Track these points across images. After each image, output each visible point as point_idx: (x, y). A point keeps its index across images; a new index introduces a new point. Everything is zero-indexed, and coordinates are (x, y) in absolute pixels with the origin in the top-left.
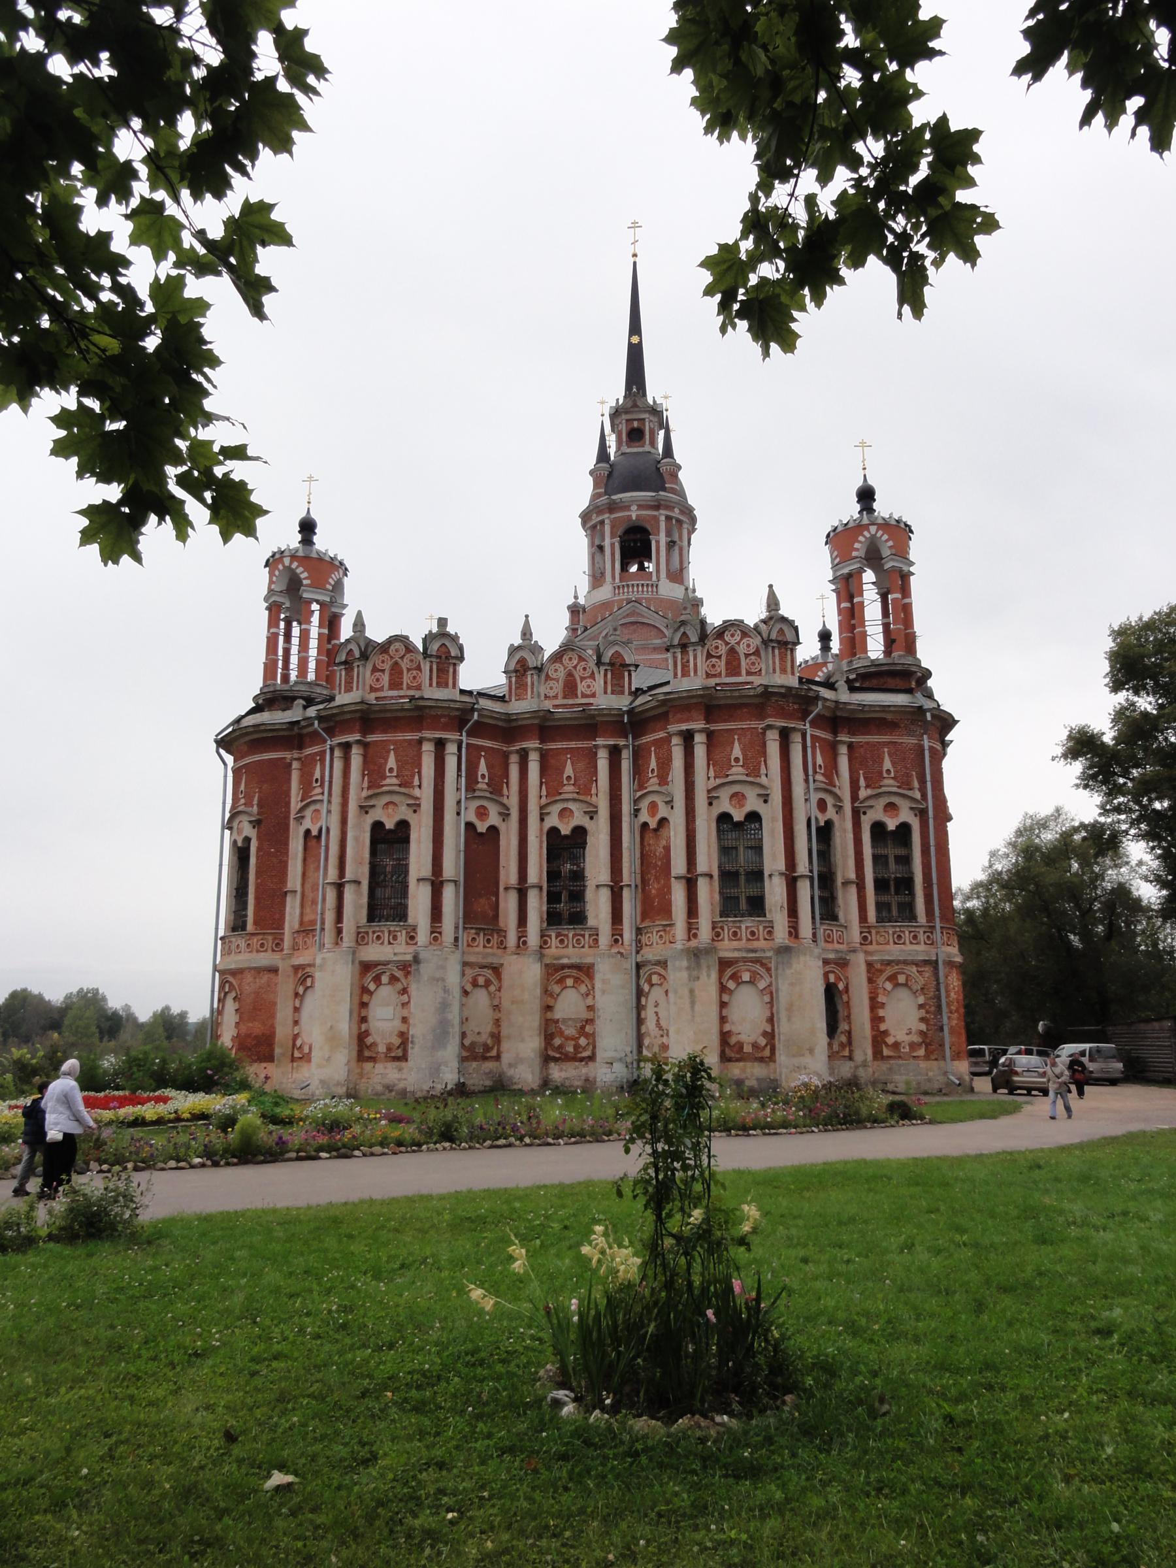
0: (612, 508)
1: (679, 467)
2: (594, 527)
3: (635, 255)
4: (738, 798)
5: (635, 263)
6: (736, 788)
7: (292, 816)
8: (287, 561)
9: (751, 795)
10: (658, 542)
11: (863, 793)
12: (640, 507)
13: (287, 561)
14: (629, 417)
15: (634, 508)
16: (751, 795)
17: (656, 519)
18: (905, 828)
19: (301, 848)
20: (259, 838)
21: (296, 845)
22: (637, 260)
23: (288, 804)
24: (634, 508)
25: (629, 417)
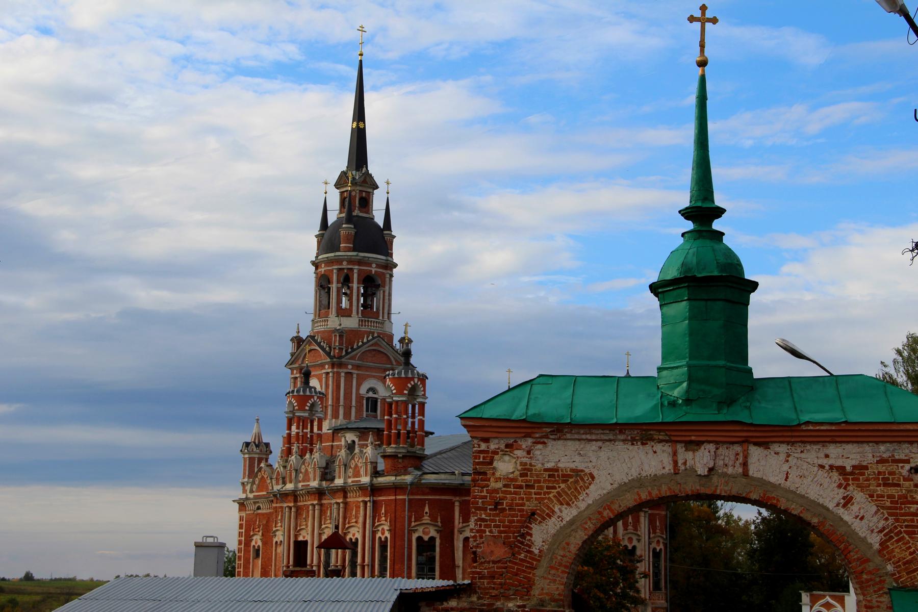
0: (360, 262)
1: (394, 237)
2: (340, 270)
3: (361, 55)
4: (630, 540)
5: (361, 61)
6: (630, 535)
7: (456, 530)
8: (416, 380)
9: (635, 538)
10: (384, 292)
11: (652, 536)
12: (378, 266)
13: (416, 380)
14: (361, 188)
15: (374, 265)
16: (635, 538)
17: (384, 274)
18: (661, 550)
19: (461, 545)
20: (440, 538)
21: (459, 545)
22: (363, 58)
23: (453, 522)
24: (374, 265)
25: (361, 188)
